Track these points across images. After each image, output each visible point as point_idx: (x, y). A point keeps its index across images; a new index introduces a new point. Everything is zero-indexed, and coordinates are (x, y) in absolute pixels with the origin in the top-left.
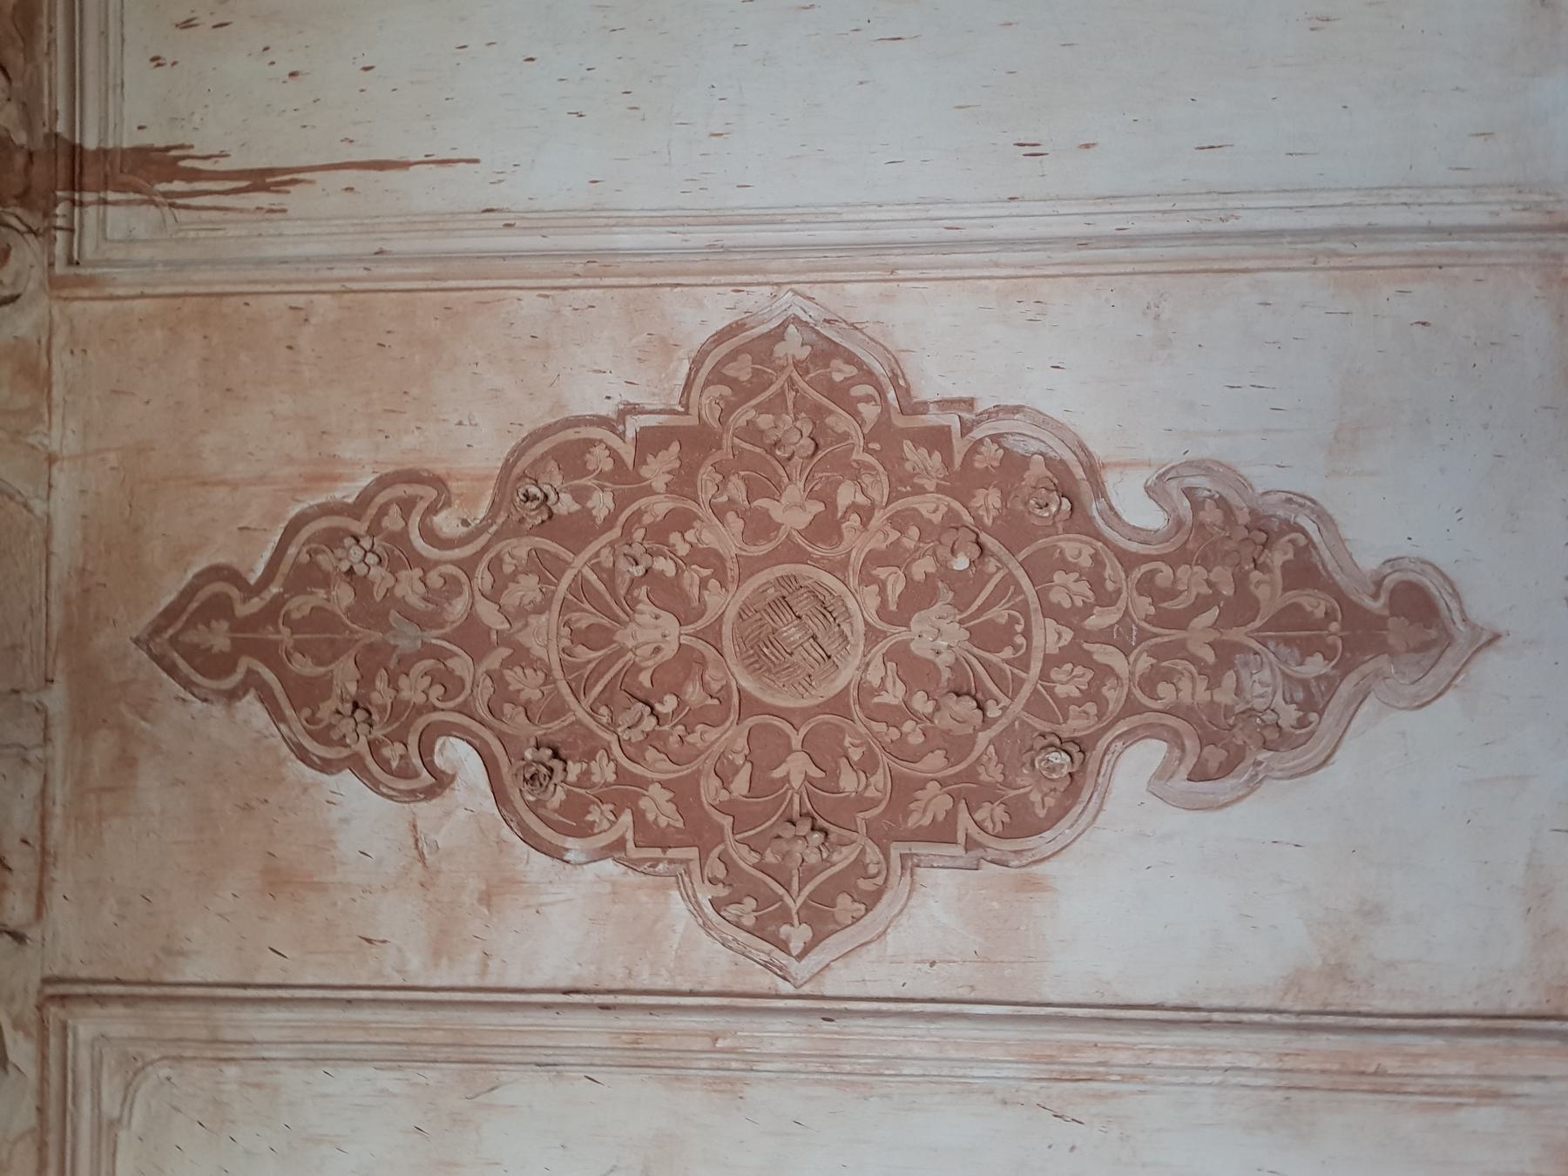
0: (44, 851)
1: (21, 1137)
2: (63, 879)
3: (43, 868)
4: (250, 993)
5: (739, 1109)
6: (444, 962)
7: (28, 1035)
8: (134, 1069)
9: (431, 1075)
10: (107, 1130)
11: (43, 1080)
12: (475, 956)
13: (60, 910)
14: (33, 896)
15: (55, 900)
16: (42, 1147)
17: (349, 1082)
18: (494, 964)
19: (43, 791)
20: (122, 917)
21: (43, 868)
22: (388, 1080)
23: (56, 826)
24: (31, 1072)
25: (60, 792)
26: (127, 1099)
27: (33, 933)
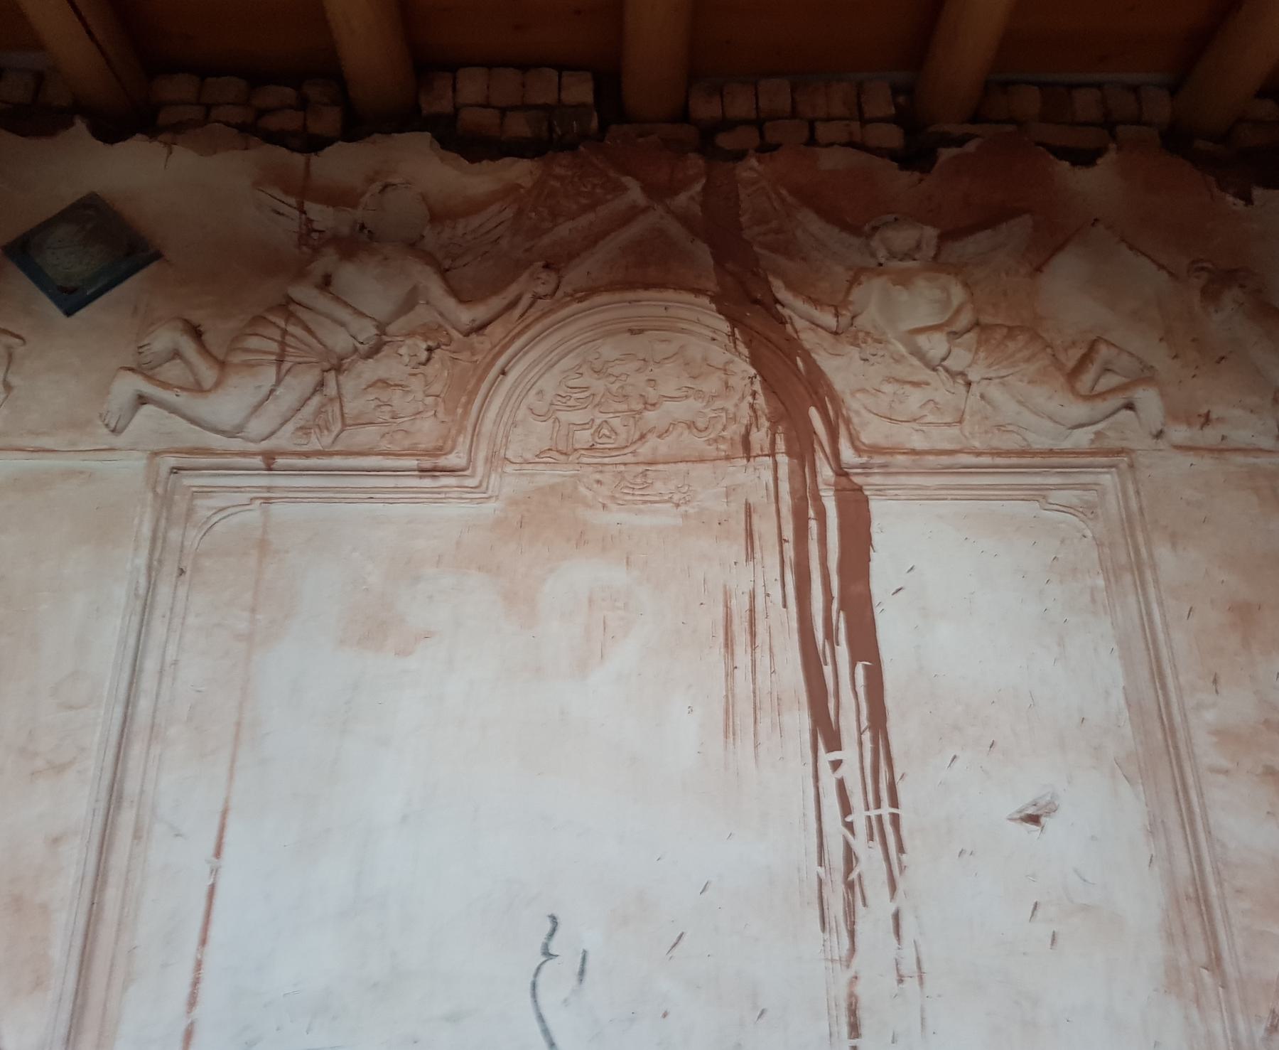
0: (1221, 451)
1: (1025, 439)
2: (1206, 463)
3: (1211, 450)
4: (1177, 775)
5: (1156, 990)
6: (1215, 739)
7: (1092, 441)
8: (1088, 511)
9: (1128, 730)
10: (1039, 494)
11: (1062, 453)
12: (1224, 763)
13: (1183, 462)
14: (1190, 443)
15: (1191, 458)
16: (1022, 453)
17: (1110, 671)
18: (1221, 778)
19: (1261, 450)
20: (1188, 503)
21: (1211, 450)
22: (1118, 699)
23: (1239, 459)
24: (1067, 445)
25: (1263, 461)
26: (1067, 508)
27: (1162, 444)
